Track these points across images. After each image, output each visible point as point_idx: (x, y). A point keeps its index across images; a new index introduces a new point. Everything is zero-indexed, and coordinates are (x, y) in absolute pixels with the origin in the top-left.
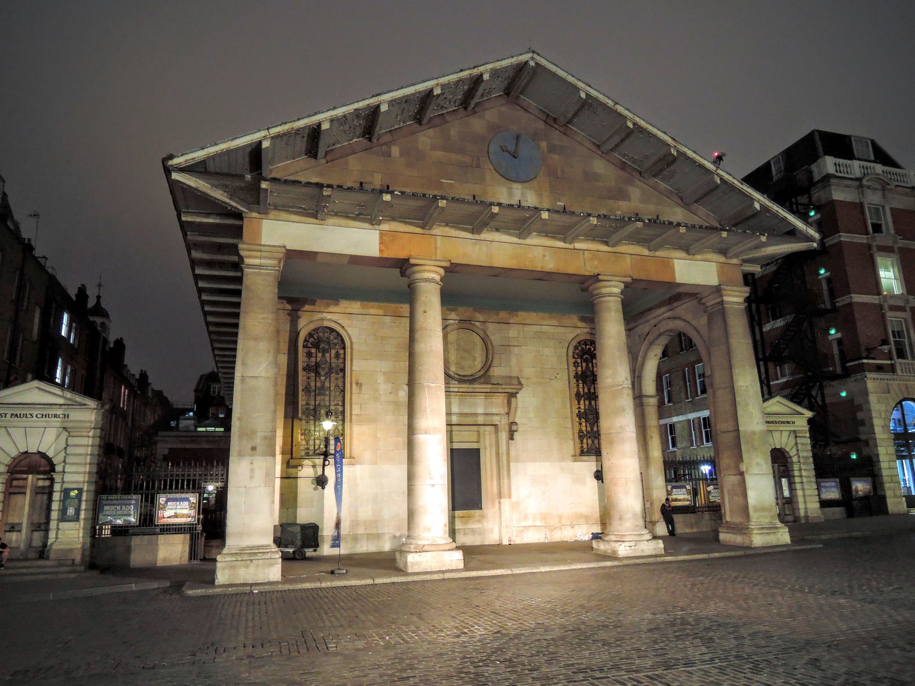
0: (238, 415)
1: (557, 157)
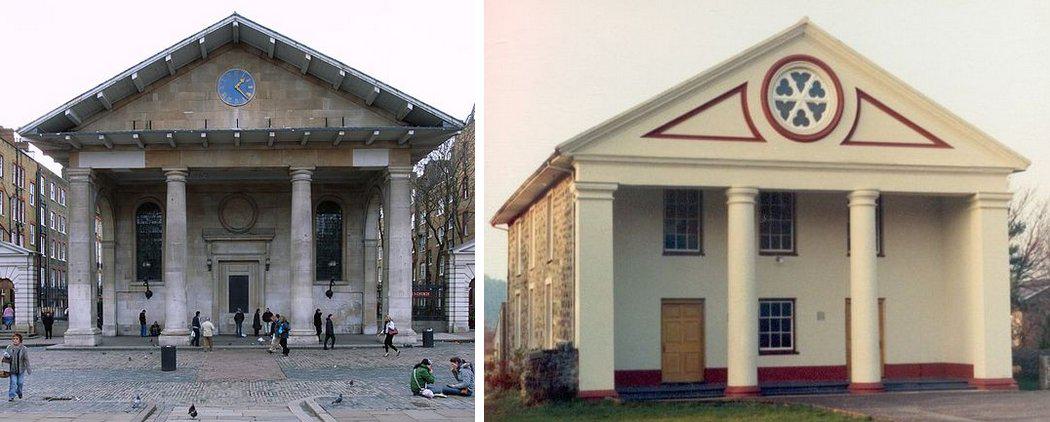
1: (267, 83)
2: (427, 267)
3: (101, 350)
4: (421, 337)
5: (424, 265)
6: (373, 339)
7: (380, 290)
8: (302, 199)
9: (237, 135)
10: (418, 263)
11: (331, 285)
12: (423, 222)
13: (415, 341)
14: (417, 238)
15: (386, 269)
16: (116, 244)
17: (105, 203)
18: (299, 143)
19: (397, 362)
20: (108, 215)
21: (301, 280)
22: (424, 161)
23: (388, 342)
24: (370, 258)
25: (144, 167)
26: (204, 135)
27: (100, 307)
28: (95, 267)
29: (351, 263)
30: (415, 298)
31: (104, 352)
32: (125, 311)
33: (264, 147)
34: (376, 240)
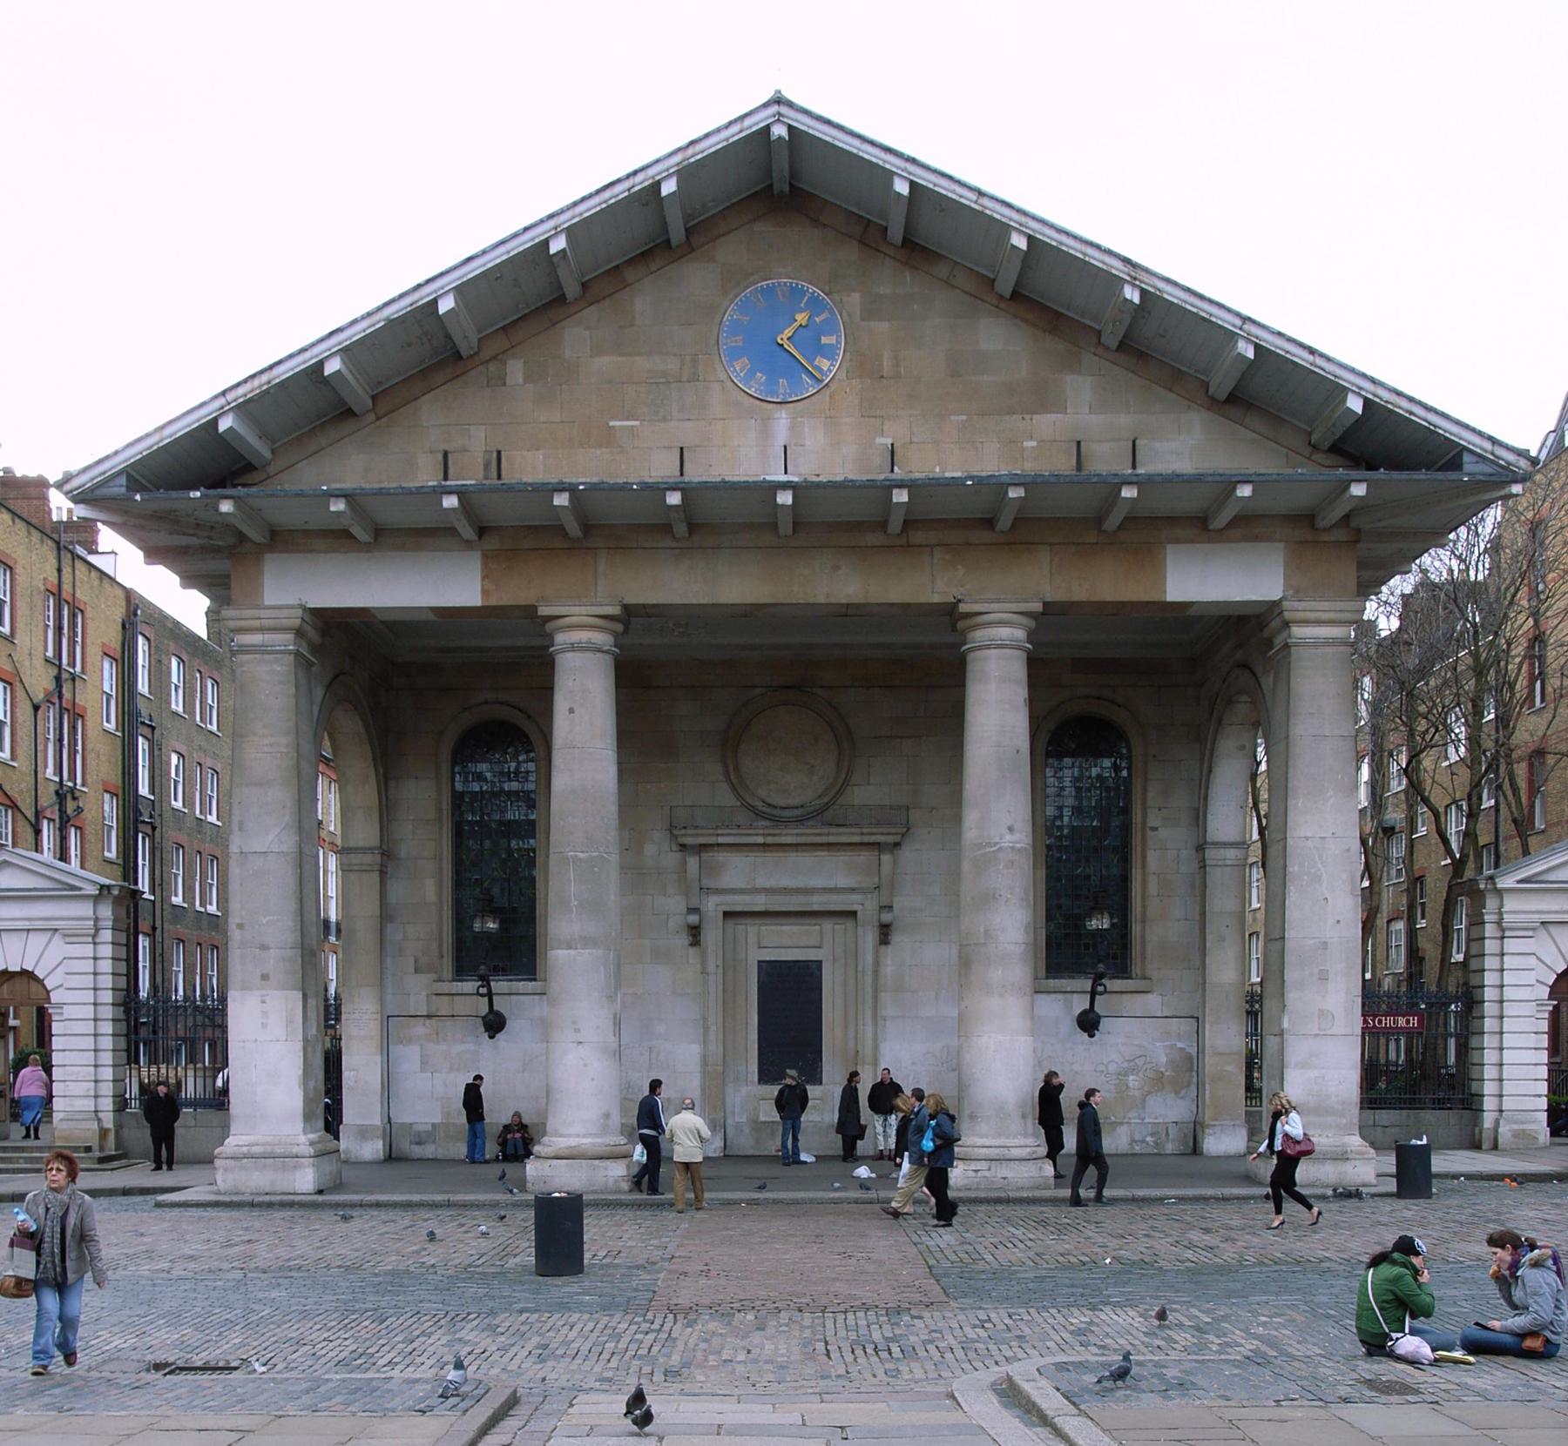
0: (238, 921)
2: (1412, 933)
3: (337, 1205)
4: (1389, 1163)
5: (1400, 926)
6: (1232, 1171)
7: (1256, 1009)
8: (997, 711)
9: (785, 498)
10: (1381, 921)
11: (1093, 994)
12: (1397, 785)
13: (1372, 1178)
14: (1378, 836)
15: (1276, 937)
16: (386, 857)
17: (350, 724)
18: (989, 523)
19: (1312, 1246)
20: (360, 764)
21: (996, 975)
22: (1401, 584)
23: (1283, 1184)
24: (1221, 902)
25: (479, 604)
26: (674, 499)
27: (332, 1064)
28: (314, 930)
29: (1159, 918)
30: (1371, 1035)
31: (346, 1211)
32: (415, 1077)
33: (873, 539)
34: (1243, 845)
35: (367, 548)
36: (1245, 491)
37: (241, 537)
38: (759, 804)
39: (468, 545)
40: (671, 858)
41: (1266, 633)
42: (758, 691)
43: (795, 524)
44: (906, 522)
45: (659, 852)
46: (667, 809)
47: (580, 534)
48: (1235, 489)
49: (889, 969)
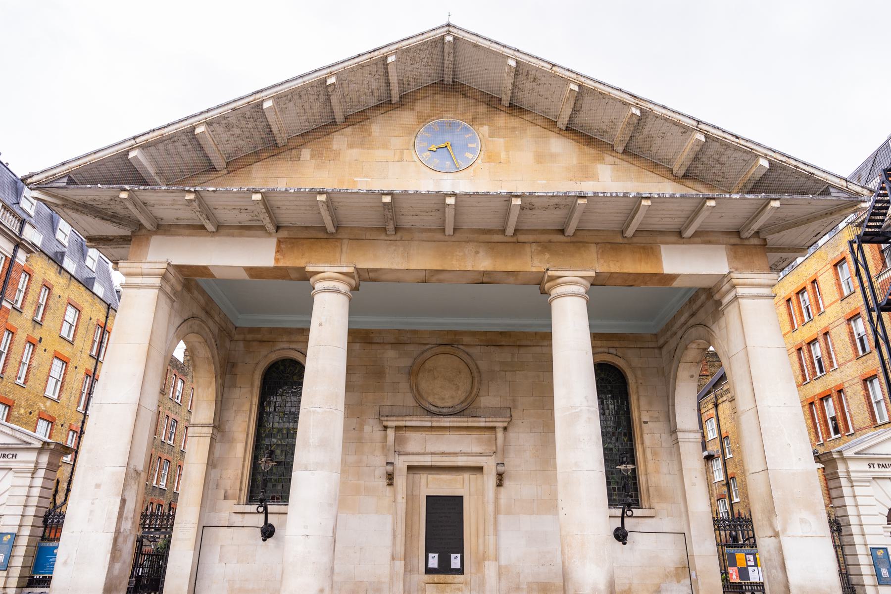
9: (451, 201)
35: (213, 234)
36: (712, 203)
37: (141, 226)
38: (428, 406)
39: (269, 234)
40: (378, 434)
41: (717, 297)
42: (429, 346)
43: (455, 230)
44: (516, 230)
45: (371, 429)
46: (378, 408)
47: (333, 231)
48: (705, 202)
49: (503, 501)
